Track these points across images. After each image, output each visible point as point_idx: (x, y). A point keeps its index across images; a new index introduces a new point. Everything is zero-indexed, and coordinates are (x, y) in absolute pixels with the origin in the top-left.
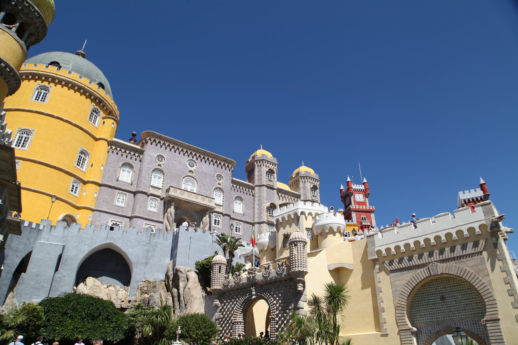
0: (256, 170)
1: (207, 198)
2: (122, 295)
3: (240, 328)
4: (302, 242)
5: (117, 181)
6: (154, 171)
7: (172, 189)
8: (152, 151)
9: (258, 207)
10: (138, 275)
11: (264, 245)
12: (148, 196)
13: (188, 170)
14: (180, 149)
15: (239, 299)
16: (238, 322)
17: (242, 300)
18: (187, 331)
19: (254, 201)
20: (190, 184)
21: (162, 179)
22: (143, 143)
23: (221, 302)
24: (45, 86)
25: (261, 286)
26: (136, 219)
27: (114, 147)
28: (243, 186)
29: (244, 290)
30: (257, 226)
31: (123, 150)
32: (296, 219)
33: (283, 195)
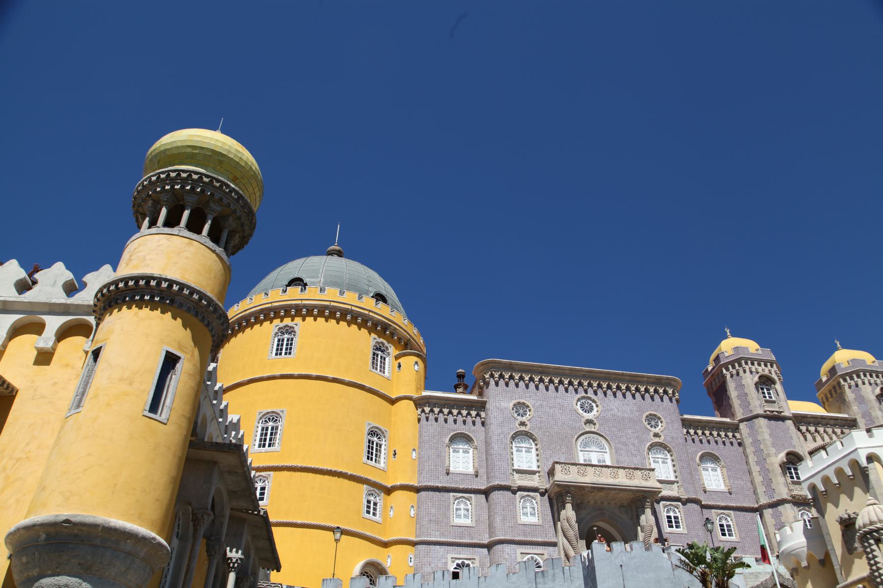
0: (731, 385)
1: (639, 473)
5: (448, 474)
6: (513, 438)
8: (500, 399)
9: (758, 468)
12: (514, 492)
13: (583, 420)
14: (556, 381)
19: (747, 457)
20: (594, 448)
21: (534, 451)
22: (481, 388)
26: (499, 547)
28: (711, 429)
30: (768, 513)
31: (446, 411)
33: (812, 429)
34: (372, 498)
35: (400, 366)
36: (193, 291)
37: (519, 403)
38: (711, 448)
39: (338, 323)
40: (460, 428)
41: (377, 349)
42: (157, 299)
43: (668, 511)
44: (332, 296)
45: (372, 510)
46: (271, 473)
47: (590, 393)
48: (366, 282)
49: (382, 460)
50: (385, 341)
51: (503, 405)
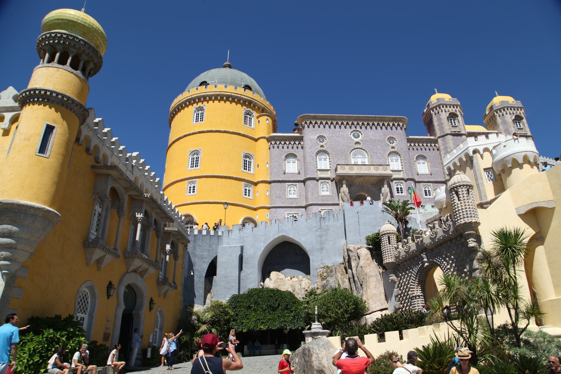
1: (381, 167)
2: (305, 284)
3: (420, 302)
4: (464, 185)
5: (285, 174)
6: (317, 154)
7: (339, 167)
8: (310, 134)
10: (315, 263)
11: (441, 203)
12: (318, 181)
13: (354, 142)
14: (361, 123)
15: (413, 270)
16: (415, 296)
17: (416, 270)
18: (327, 311)
19: (441, 156)
20: (359, 156)
21: (328, 159)
23: (397, 276)
24: (200, 107)
25: (432, 250)
26: (310, 207)
27: (273, 143)
28: (423, 143)
29: (416, 258)
31: (283, 143)
32: (468, 162)
34: (247, 188)
35: (259, 122)
36: (58, 94)
40: (291, 151)
41: (247, 114)
42: (40, 100)
43: (397, 185)
44: (221, 89)
45: (247, 194)
46: (197, 179)
47: (358, 127)
48: (240, 80)
49: (252, 169)
50: (251, 110)
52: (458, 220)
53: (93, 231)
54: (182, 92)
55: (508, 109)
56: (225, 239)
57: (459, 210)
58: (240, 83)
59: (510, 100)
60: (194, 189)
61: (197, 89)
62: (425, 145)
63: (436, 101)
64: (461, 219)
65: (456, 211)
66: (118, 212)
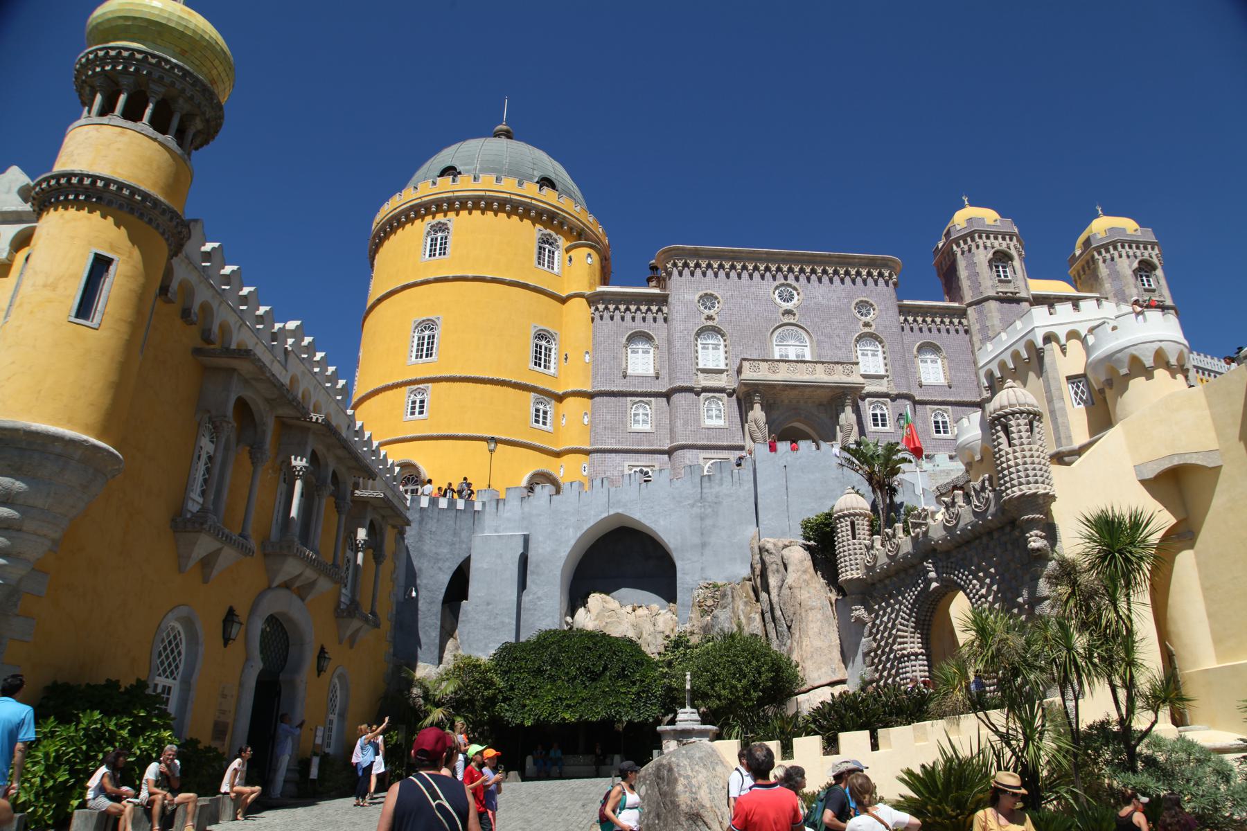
0: (962, 264)
1: (840, 367)
2: (665, 622)
3: (917, 668)
4: (1021, 413)
5: (625, 377)
6: (698, 334)
7: (746, 364)
8: (685, 291)
10: (688, 576)
11: (971, 449)
12: (698, 394)
13: (781, 311)
14: (797, 269)
15: (904, 598)
16: (908, 656)
17: (910, 596)
18: (712, 684)
19: (972, 345)
20: (792, 342)
23: (869, 610)
25: (948, 553)
26: (680, 452)
27: (601, 307)
28: (933, 315)
29: (912, 571)
31: (622, 307)
32: (1031, 361)
34: (541, 407)
35: (570, 260)
36: (121, 186)
37: (706, 294)
38: (933, 338)
39: (496, 215)
40: (639, 326)
41: (544, 242)
42: (82, 198)
43: (874, 409)
44: (487, 184)
45: (541, 419)
47: (791, 280)
49: (552, 365)
50: (552, 233)
51: (688, 297)
52: (1007, 489)
53: (195, 495)
54: (400, 188)
55: (1123, 247)
56: (489, 519)
57: (1010, 467)
58: (530, 171)
59: (1128, 225)
60: (422, 407)
61: (434, 183)
62: (938, 320)
63: (965, 225)
64: (1013, 486)
65: (1003, 469)
66: (250, 453)
